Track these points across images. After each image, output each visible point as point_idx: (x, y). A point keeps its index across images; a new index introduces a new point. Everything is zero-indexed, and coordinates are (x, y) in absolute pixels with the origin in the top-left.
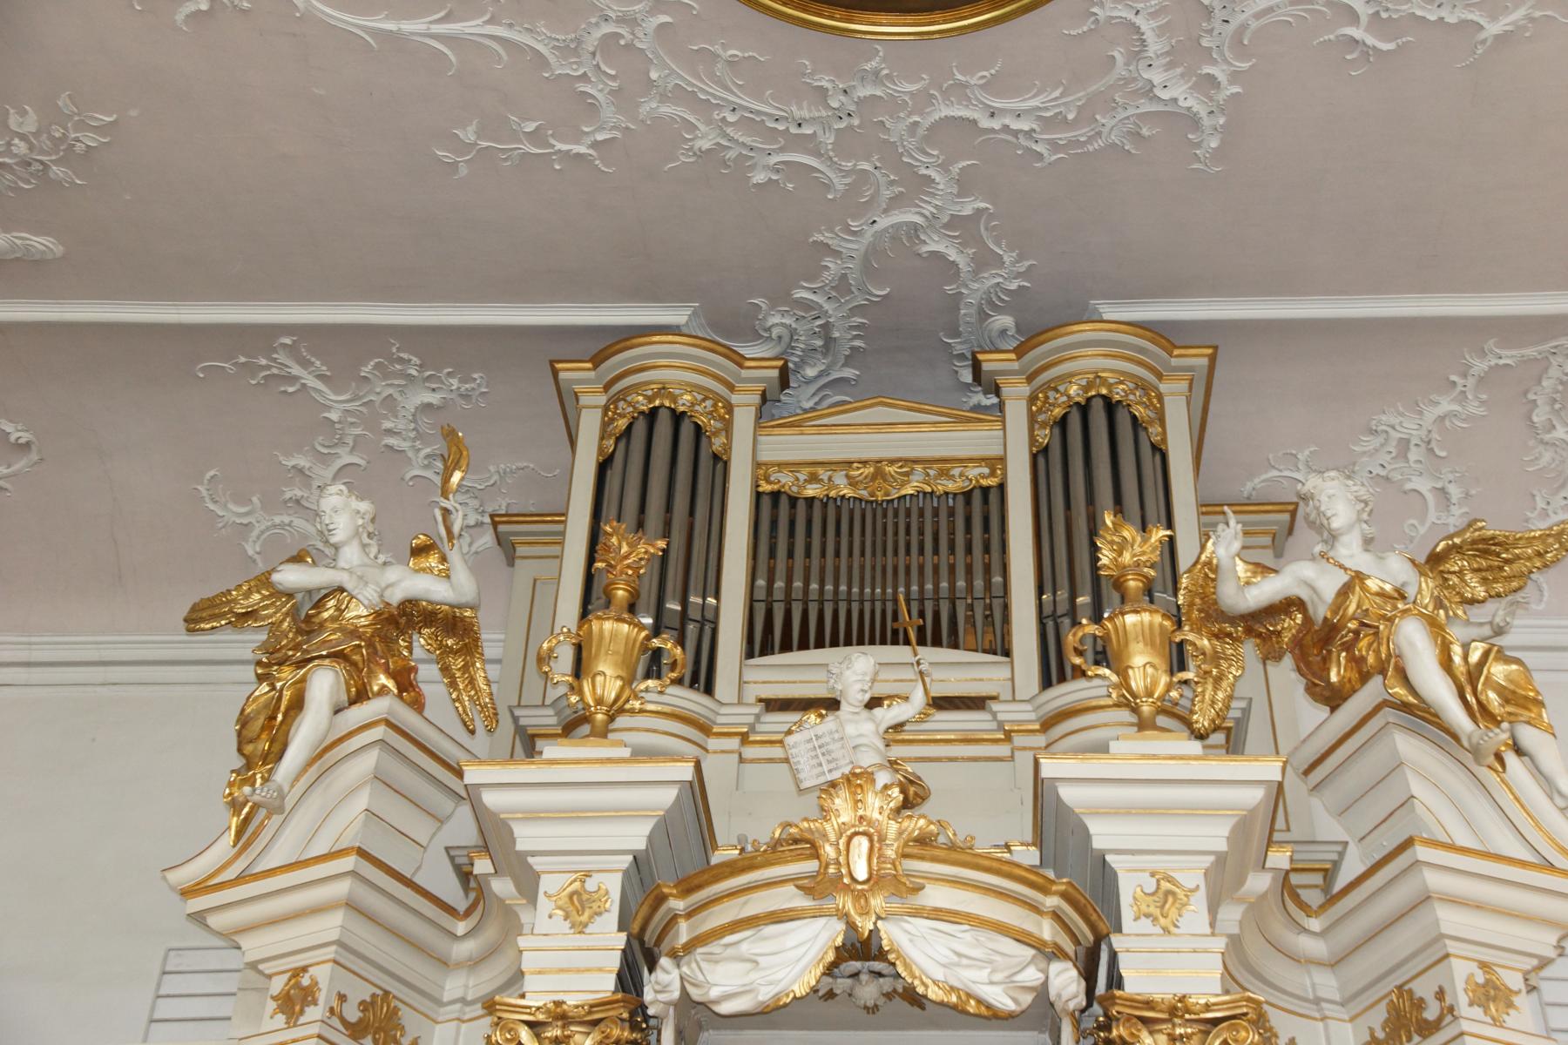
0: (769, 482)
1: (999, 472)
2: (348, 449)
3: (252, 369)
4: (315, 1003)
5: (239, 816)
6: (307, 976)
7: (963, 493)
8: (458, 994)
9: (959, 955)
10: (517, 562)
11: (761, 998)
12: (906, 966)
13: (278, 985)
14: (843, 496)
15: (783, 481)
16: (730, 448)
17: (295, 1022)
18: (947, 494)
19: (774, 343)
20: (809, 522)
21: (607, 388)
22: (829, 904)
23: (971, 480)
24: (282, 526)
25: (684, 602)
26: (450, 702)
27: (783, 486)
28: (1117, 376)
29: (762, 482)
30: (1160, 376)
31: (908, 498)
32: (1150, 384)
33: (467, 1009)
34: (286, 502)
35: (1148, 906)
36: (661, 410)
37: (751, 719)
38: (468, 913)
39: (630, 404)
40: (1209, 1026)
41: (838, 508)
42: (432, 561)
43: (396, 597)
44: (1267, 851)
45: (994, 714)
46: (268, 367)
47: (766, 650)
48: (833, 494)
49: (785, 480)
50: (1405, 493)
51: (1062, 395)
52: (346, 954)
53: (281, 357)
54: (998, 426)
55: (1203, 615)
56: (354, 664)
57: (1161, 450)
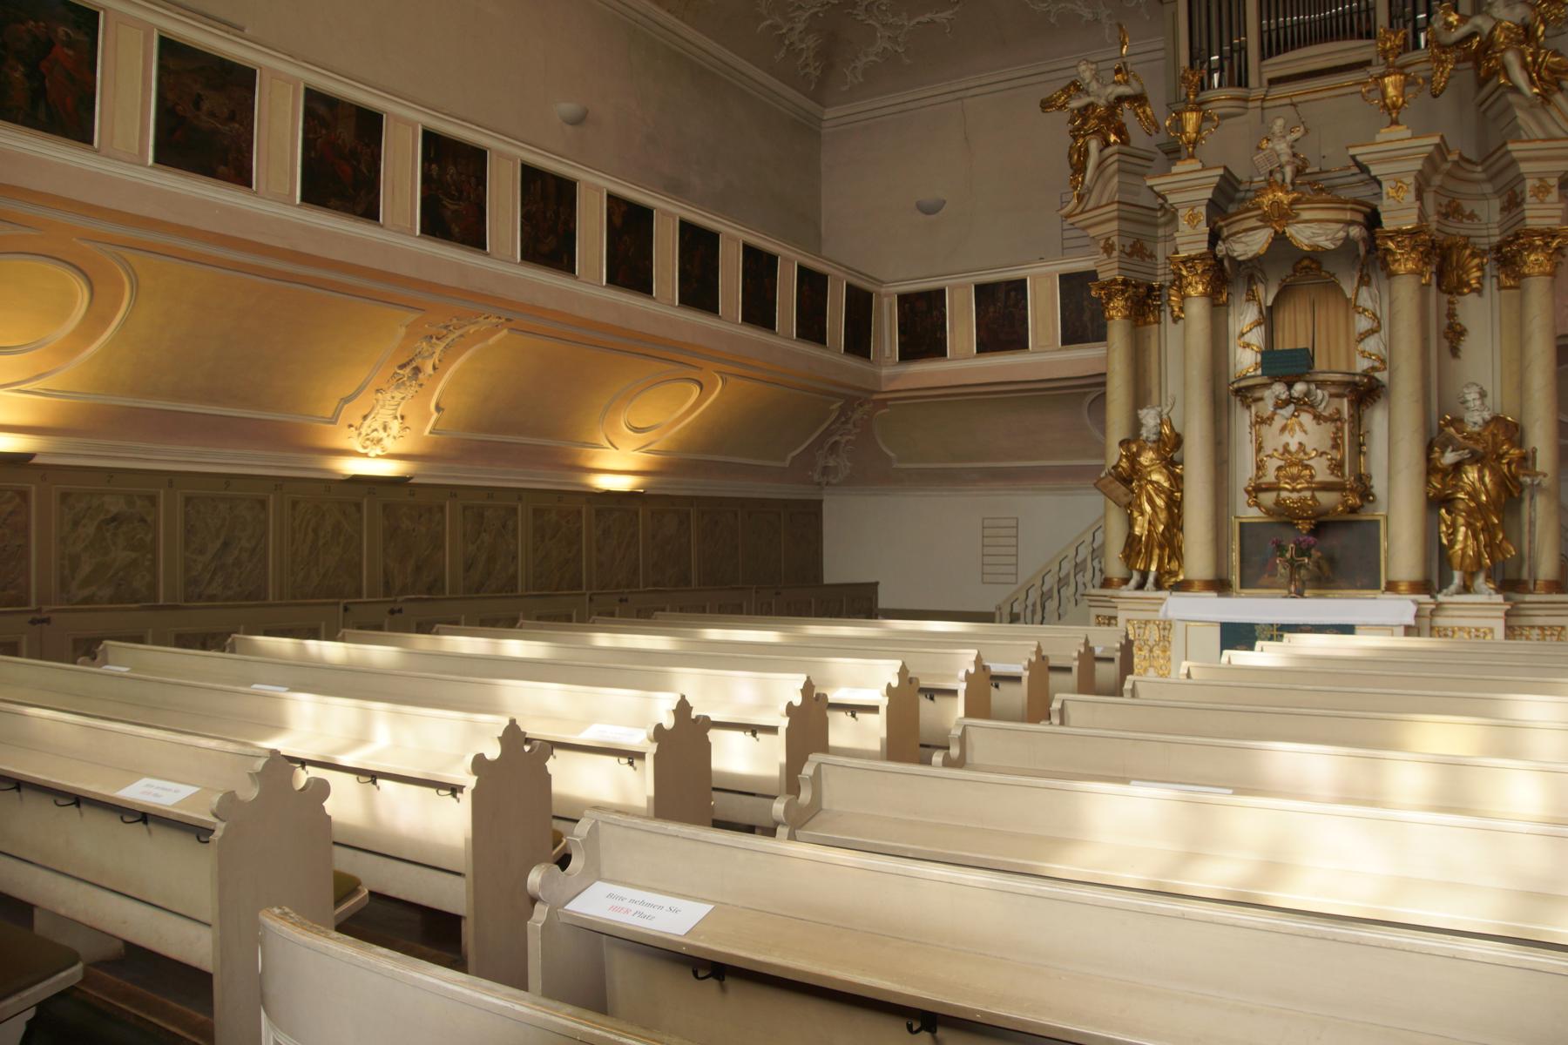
8: (1163, 234)
9: (1313, 233)
22: (1269, 224)
24: (1063, 8)
25: (1231, 44)
37: (1263, 93)
38: (1160, 210)
43: (1112, 98)
45: (1368, 72)
47: (1270, 56)
52: (1121, 233)
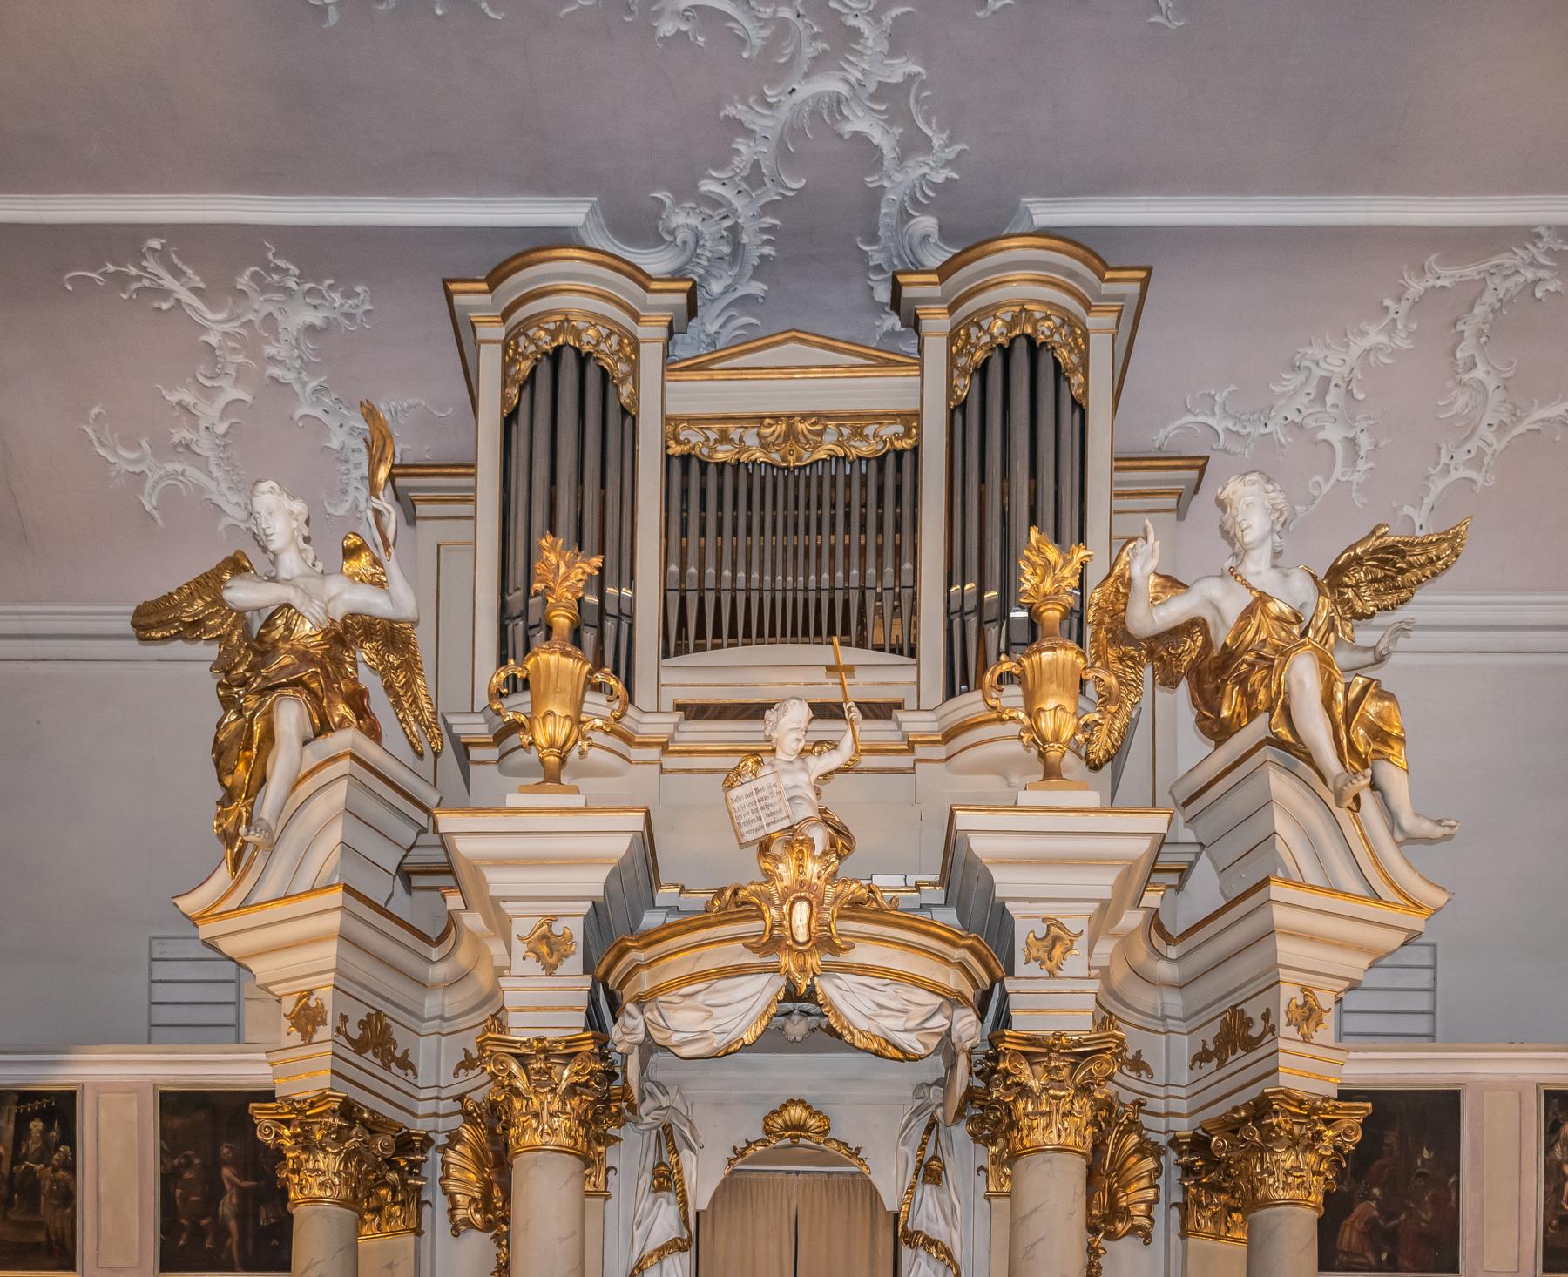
0: (678, 442)
1: (914, 431)
2: (231, 381)
3: (121, 280)
4: (324, 1023)
5: (232, 849)
6: (313, 998)
7: (877, 458)
10: (419, 523)
11: (715, 1045)
12: (838, 1018)
13: (289, 1005)
14: (754, 462)
15: (693, 440)
16: (638, 399)
17: (310, 1041)
18: (860, 458)
19: (676, 250)
20: (720, 491)
21: (505, 315)
23: (885, 442)
26: (398, 723)
27: (693, 448)
28: (1043, 308)
29: (672, 443)
30: (1088, 307)
31: (820, 463)
32: (1077, 318)
33: (446, 1024)
34: (175, 446)
35: (1038, 951)
36: (564, 349)
39: (531, 340)
40: (1079, 1057)
41: (750, 476)
42: (362, 563)
44: (1145, 890)
46: (139, 278)
48: (744, 458)
49: (694, 437)
50: (1316, 443)
51: (985, 333)
53: (152, 265)
54: (915, 371)
55: (1110, 635)
56: (312, 692)
57: (1081, 406)
